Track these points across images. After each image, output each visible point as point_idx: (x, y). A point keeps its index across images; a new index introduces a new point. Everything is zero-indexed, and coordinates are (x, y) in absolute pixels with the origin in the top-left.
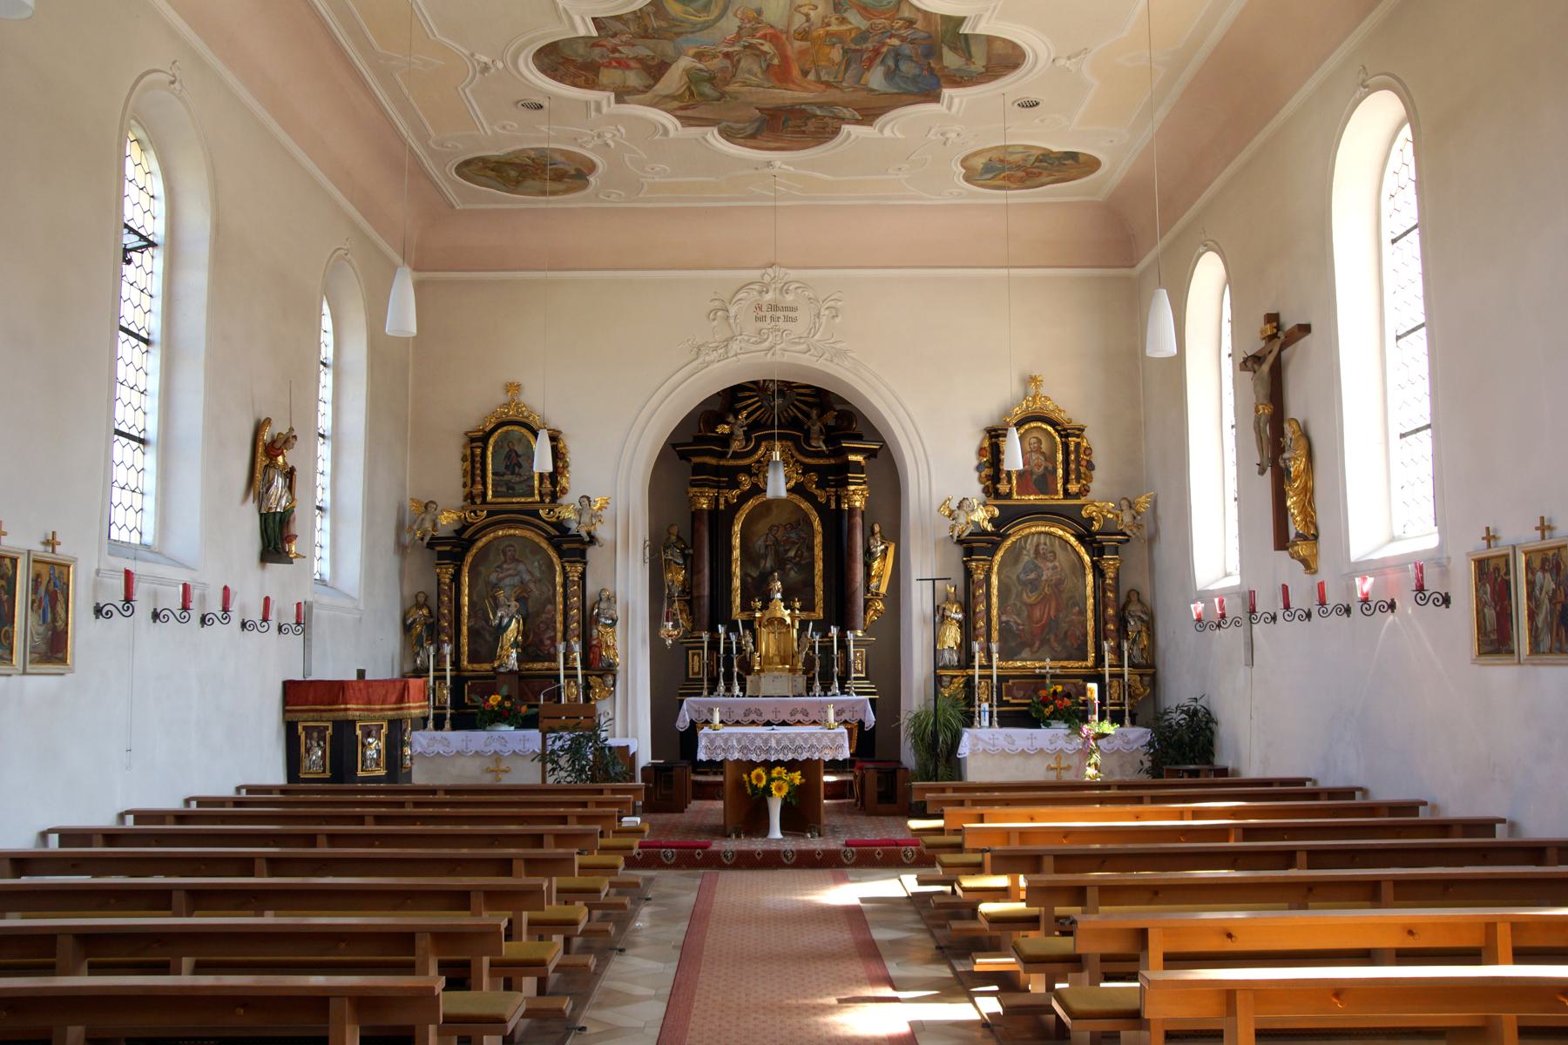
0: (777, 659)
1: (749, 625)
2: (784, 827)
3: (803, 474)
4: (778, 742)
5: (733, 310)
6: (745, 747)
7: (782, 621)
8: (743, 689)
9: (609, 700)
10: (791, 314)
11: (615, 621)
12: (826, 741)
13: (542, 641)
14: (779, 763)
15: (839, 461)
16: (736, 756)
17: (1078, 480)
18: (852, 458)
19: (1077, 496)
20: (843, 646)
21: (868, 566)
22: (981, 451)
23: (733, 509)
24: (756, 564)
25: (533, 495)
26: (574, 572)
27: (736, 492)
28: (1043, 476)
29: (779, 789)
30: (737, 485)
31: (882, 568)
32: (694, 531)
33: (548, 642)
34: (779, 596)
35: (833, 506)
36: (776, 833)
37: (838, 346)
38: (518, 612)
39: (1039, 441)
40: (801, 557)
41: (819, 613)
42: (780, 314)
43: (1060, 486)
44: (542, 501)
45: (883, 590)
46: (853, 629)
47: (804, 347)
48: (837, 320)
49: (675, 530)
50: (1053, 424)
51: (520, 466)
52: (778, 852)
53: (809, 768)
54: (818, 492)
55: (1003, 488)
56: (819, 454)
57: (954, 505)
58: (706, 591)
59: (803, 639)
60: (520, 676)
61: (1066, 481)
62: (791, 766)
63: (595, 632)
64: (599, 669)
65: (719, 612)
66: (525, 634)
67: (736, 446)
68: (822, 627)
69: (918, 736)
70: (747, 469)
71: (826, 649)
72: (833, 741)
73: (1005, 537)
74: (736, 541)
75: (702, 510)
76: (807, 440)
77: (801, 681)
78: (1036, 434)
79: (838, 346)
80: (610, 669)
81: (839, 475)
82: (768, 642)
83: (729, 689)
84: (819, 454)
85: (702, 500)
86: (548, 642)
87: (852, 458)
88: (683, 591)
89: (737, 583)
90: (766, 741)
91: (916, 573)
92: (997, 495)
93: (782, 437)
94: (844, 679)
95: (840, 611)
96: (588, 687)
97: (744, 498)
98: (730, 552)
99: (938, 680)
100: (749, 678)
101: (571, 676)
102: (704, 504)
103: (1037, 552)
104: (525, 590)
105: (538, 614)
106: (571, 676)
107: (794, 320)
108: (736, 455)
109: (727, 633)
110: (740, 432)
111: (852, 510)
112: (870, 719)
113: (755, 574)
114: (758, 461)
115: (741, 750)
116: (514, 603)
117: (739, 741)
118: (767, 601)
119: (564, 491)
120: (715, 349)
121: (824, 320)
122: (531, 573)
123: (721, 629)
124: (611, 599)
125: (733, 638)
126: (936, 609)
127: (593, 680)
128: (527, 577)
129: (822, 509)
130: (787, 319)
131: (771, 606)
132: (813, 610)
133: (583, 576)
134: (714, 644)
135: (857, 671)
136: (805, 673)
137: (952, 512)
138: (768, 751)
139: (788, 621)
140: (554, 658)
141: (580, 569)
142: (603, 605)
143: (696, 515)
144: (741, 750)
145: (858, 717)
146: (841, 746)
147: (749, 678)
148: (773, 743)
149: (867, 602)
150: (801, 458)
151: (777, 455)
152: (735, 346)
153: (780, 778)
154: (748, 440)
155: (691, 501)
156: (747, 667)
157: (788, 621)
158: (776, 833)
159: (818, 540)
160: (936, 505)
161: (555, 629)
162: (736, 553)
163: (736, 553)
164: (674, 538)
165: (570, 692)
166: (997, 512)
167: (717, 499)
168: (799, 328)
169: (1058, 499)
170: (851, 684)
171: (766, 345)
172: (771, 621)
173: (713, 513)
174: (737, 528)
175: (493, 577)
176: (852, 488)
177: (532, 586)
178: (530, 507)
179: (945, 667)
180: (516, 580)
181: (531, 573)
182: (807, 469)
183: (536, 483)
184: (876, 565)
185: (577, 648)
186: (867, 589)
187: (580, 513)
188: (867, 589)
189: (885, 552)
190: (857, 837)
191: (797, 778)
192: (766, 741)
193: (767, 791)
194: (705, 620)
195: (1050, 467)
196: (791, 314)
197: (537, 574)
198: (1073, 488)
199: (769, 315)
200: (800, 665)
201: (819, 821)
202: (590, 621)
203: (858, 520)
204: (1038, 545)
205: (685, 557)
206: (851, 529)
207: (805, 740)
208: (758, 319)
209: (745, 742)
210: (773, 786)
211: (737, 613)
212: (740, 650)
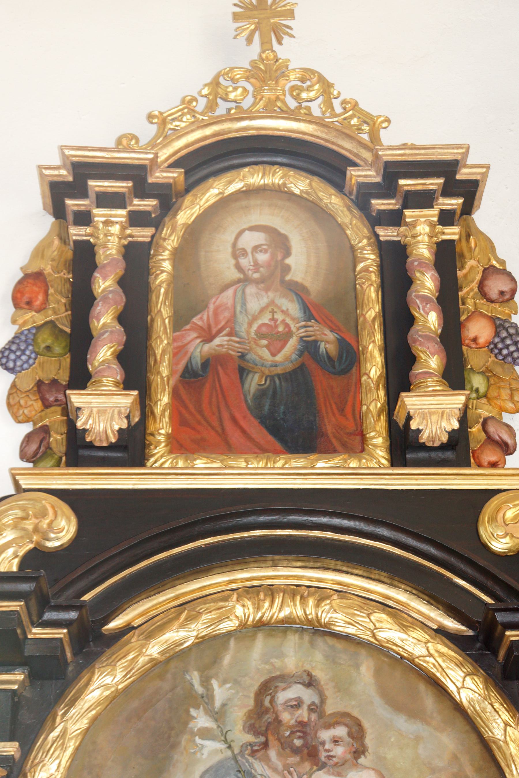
17: (454, 376)
19: (456, 450)
22: (28, 290)
28: (297, 380)
39: (280, 243)
43: (374, 401)
50: (324, 162)
55: (103, 409)
61: (400, 375)
73: (93, 642)
78: (264, 215)
92: (79, 450)
103: (263, 722)
166: (63, 530)
169: (372, 471)
195: (328, 342)
198: (433, 411)
204: (267, 688)
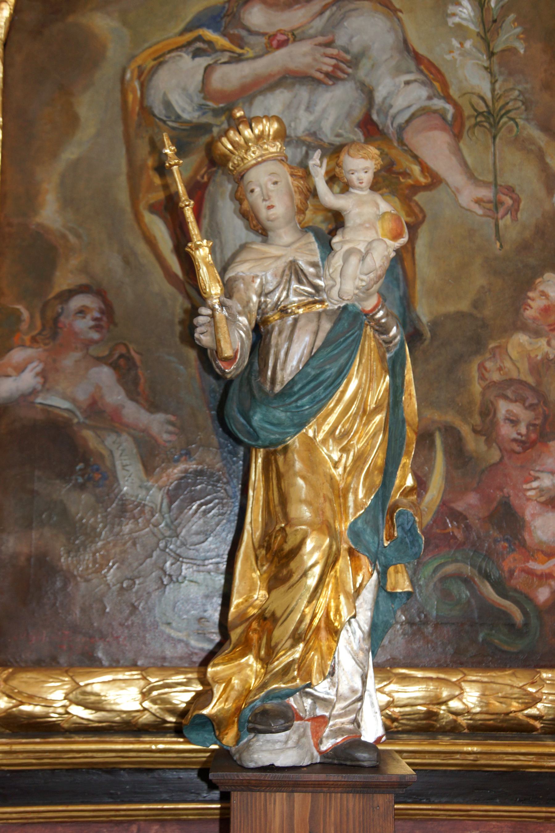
122: (430, 72)
175: (179, 85)
177: (435, 148)
181: (430, 72)
197: (472, 77)
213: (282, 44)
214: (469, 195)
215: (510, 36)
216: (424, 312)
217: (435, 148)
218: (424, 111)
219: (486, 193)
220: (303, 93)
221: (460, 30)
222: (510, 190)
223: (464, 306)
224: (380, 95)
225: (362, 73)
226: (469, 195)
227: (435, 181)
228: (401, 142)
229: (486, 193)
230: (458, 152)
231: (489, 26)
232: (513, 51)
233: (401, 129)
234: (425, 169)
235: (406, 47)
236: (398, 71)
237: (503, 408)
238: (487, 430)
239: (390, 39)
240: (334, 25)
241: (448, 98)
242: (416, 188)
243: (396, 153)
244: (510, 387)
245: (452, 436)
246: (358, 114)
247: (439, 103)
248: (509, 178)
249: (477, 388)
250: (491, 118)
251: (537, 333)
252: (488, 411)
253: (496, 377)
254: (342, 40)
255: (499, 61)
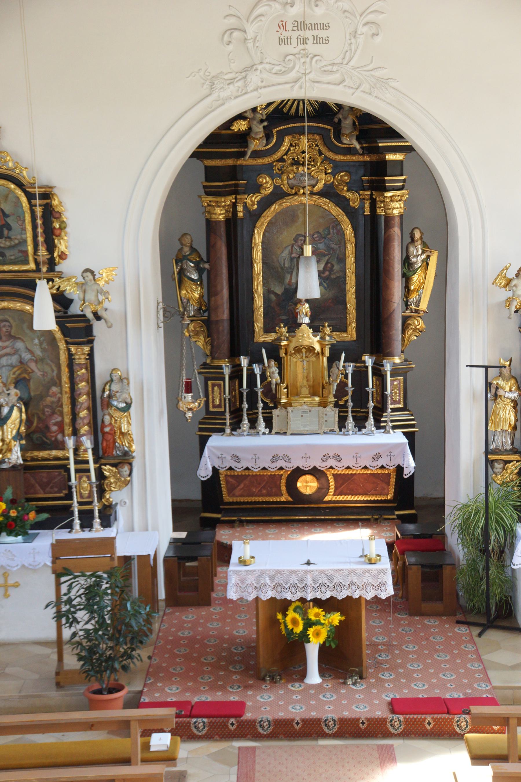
0: (305, 391)
1: (274, 350)
2: (322, 672)
3: (334, 174)
4: (315, 579)
5: (251, 30)
6: (280, 585)
7: (311, 349)
8: (269, 423)
9: (126, 490)
10: (322, 34)
11: (128, 406)
12: (367, 579)
13: (47, 428)
14: (317, 602)
15: (375, 158)
16: (268, 594)
18: (390, 157)
20: (378, 373)
21: (407, 279)
23: (254, 217)
24: (280, 279)
25: (27, 262)
26: (80, 353)
27: (256, 198)
29: (317, 634)
30: (257, 188)
31: (425, 282)
32: (210, 246)
33: (54, 428)
34: (307, 320)
35: (367, 212)
36: (314, 677)
37: (378, 73)
38: (20, 399)
40: (331, 270)
41: (351, 334)
42: (309, 34)
44: (38, 270)
45: (424, 306)
46: (390, 355)
47: (336, 77)
48: (378, 40)
49: (187, 240)
51: (9, 228)
52: (319, 720)
53: (347, 606)
54: (349, 195)
56: (350, 151)
57: (511, 274)
58: (225, 314)
59: (334, 370)
60: (27, 468)
62: (329, 605)
63: (107, 418)
64: (113, 456)
65: (238, 341)
66: (29, 422)
67: (255, 145)
68: (354, 357)
69: (465, 528)
70: (268, 169)
71: (360, 376)
72: (375, 577)
74: (258, 255)
75: (218, 222)
76: (338, 136)
77: (333, 414)
79: (378, 73)
80: (125, 460)
81: (376, 175)
82: (298, 368)
83: (253, 424)
84: (350, 151)
85: (218, 211)
86: (54, 428)
87: (390, 157)
88: (200, 309)
89: (259, 301)
90: (302, 579)
91: (465, 359)
93: (312, 131)
94: (380, 411)
95: (375, 336)
96: (101, 476)
97: (266, 204)
98: (252, 266)
99: (489, 463)
100: (275, 412)
101: (83, 471)
102: (220, 214)
104: (25, 371)
105: (41, 397)
106: (83, 471)
107: (325, 41)
108: (256, 154)
109: (250, 364)
110: (259, 129)
111: (389, 219)
112: (410, 464)
113: (279, 290)
114: (281, 160)
115: (275, 587)
116: (14, 392)
117: (272, 578)
118: (294, 325)
119: (63, 256)
120: (231, 82)
121: (361, 39)
123: (244, 361)
124: (124, 380)
125: (257, 369)
126: (488, 385)
127: (107, 470)
128: (27, 356)
129: (352, 214)
130: (318, 40)
131: (299, 333)
132: (345, 330)
133: (91, 356)
134: (236, 374)
135: (394, 402)
136: (336, 405)
137: (509, 281)
138: (304, 588)
139: (318, 348)
140: (62, 446)
141: (87, 349)
142: (115, 387)
143: (211, 225)
144: (275, 587)
145: (396, 462)
146: (384, 584)
147: (275, 412)
148: (309, 580)
149: (405, 319)
150: (331, 155)
151: (308, 250)
152: (254, 79)
153: (318, 623)
154: (268, 136)
155: (208, 210)
156: (272, 395)
157: (318, 348)
158: (314, 677)
159: (350, 248)
160: (491, 276)
161: (61, 414)
162: (258, 267)
163: (258, 267)
164: (187, 250)
165: (82, 486)
167: (234, 205)
168: (329, 53)
170: (388, 416)
171: (293, 75)
172: (298, 350)
173: (232, 222)
174: (258, 239)
176: (389, 194)
177: (33, 366)
178: (24, 276)
179: (496, 451)
180: (14, 360)
182: (337, 167)
183: (30, 249)
184: (415, 278)
185: (87, 443)
186: (407, 305)
187: (82, 286)
188: (407, 305)
189: (426, 262)
190: (406, 693)
191: (336, 618)
192: (302, 579)
193: (304, 637)
194: (225, 347)
196: (322, 34)
197: (38, 352)
199: (295, 35)
200: (331, 399)
201: (360, 664)
202: (100, 405)
203: (396, 231)
205: (200, 271)
206: (388, 241)
207: (345, 577)
208: (283, 41)
209: (279, 579)
210: (311, 631)
211: (261, 337)
212: (263, 377)
213: (5, 348)
214: (39, 374)
215: (45, 345)
216: (32, 394)
217: (33, 366)
218: (31, 359)
219: (42, 373)
220: (9, 357)
221: (36, 345)
222: (46, 372)
223: (39, 393)
224: (23, 356)
225: (19, 353)
226: (39, 374)
227: (33, 371)
228: (27, 365)
229: (42, 373)
230: (36, 366)
231: (41, 343)
232: (45, 348)
233: (27, 362)
234: (31, 369)
235: (27, 348)
236: (26, 352)
237: (46, 410)
238: (44, 413)
239: (24, 347)
240: (13, 345)
241: (34, 357)
242: (30, 373)
243: (26, 367)
244: (47, 406)
245: (38, 414)
246: (19, 360)
247: (33, 358)
248: (46, 370)
249: (41, 407)
250: (42, 360)
251: (51, 397)
252: (43, 410)
253: (45, 404)
254: (15, 347)
255: (43, 350)
